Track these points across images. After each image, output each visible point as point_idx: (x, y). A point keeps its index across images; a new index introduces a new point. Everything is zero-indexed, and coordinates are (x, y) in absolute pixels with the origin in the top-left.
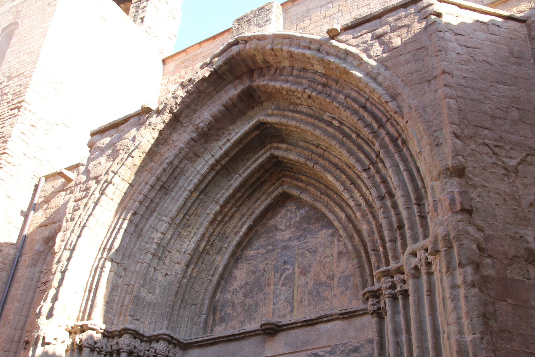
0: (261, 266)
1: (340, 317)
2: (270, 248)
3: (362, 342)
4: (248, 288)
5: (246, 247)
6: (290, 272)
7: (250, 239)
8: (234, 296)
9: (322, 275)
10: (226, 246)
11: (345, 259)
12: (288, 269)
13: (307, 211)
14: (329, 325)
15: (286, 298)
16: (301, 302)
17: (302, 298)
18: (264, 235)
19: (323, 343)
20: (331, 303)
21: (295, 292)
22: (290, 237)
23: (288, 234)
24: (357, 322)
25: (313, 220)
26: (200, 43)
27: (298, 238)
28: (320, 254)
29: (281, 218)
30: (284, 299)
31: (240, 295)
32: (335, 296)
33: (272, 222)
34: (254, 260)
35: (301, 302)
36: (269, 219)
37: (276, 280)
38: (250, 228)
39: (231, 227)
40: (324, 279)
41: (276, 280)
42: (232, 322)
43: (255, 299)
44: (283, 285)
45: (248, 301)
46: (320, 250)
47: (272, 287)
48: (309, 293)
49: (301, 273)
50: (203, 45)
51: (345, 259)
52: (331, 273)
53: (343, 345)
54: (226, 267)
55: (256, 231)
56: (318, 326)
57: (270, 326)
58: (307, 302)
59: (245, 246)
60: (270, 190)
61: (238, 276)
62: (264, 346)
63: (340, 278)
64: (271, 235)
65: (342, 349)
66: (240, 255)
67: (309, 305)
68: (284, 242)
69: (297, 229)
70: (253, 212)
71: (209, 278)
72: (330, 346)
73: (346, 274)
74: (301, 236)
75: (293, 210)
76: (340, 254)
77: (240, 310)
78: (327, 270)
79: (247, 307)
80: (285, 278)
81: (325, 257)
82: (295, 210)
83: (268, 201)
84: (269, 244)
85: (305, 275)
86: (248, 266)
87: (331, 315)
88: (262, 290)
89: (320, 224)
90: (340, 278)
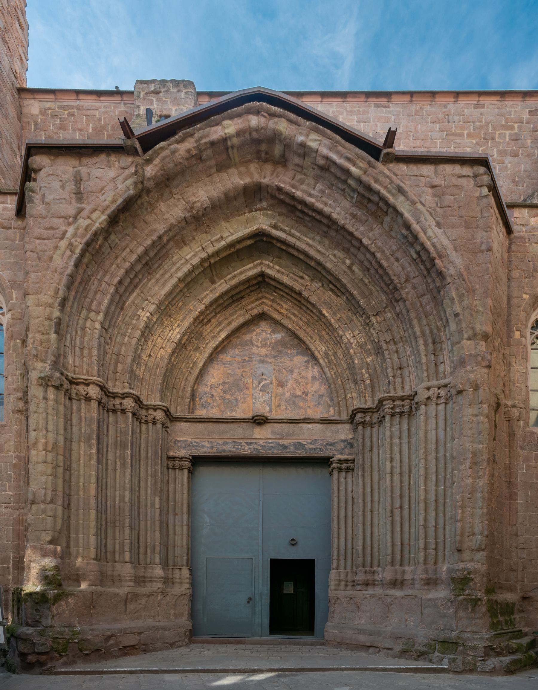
0: (238, 371)
1: (321, 422)
2: (247, 359)
3: (337, 441)
4: (227, 386)
5: (220, 352)
6: (268, 382)
7: (225, 345)
8: (213, 390)
9: (297, 390)
10: (204, 346)
11: (318, 382)
12: (266, 380)
13: (282, 336)
14: (310, 426)
15: (264, 401)
16: (279, 406)
17: (280, 404)
18: (240, 347)
19: (306, 436)
20: (306, 412)
21: (273, 398)
22: (266, 354)
23: (264, 351)
24: (333, 427)
25: (289, 346)
26: (78, 92)
27: (274, 357)
28: (296, 374)
29: (256, 335)
30: (262, 401)
31: (219, 390)
32: (309, 407)
33: (247, 337)
34: (231, 365)
35: (279, 406)
36: (243, 334)
37: (254, 385)
38: (228, 337)
39: (208, 330)
40: (299, 393)
41: (254, 385)
42: (214, 410)
43: (235, 396)
44: (261, 390)
45: (228, 396)
46: (296, 371)
47: (251, 390)
48: (286, 401)
49: (278, 385)
50: (81, 97)
51: (318, 382)
52: (306, 390)
53: (322, 440)
54: (205, 364)
55: (230, 341)
56: (301, 425)
57: (262, 418)
58: (284, 407)
59: (220, 351)
60: (249, 307)
61: (215, 374)
62: (253, 431)
63: (313, 395)
64: (247, 348)
65: (321, 442)
66: (215, 357)
67: (286, 409)
68: (261, 356)
69: (273, 349)
70: (230, 323)
71: (189, 369)
72: (311, 439)
73: (320, 393)
74: (277, 356)
75: (269, 332)
76: (314, 378)
77: (219, 402)
78: (302, 388)
79: (226, 401)
80: (262, 386)
81: (301, 378)
82: (271, 332)
83: (247, 317)
84: (245, 355)
85: (282, 387)
86: (226, 369)
87: (313, 419)
88: (241, 390)
89: (295, 351)
90: (313, 395)
